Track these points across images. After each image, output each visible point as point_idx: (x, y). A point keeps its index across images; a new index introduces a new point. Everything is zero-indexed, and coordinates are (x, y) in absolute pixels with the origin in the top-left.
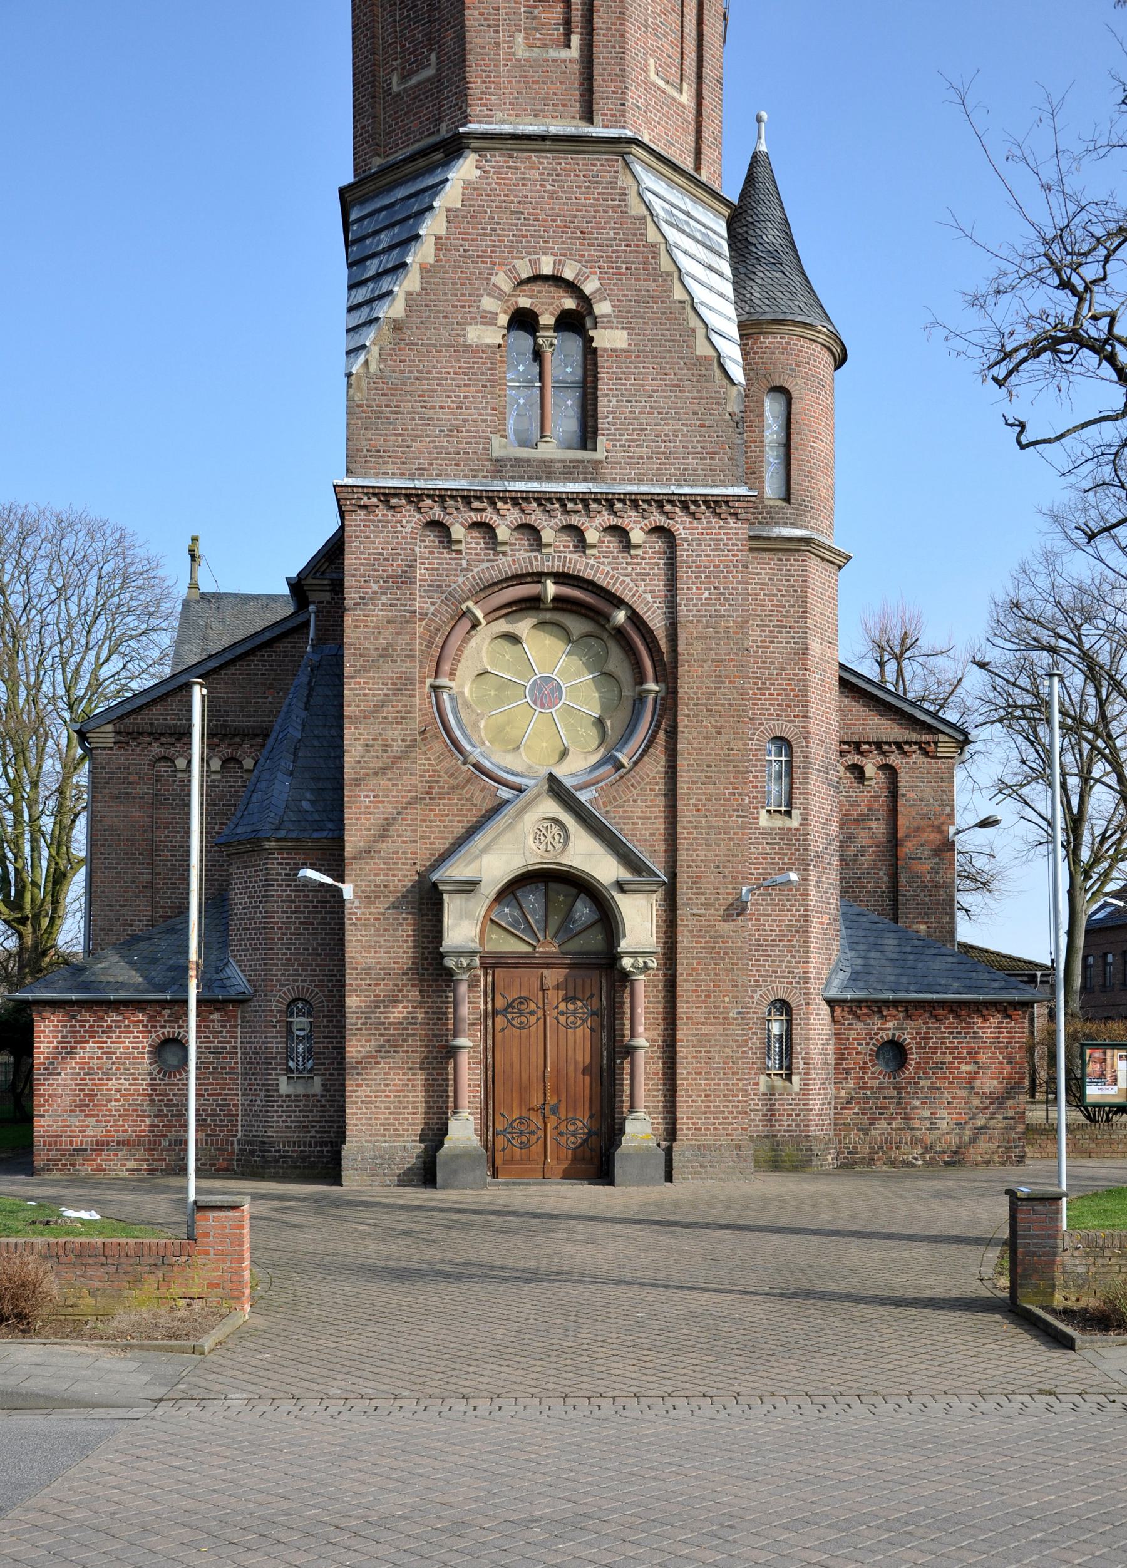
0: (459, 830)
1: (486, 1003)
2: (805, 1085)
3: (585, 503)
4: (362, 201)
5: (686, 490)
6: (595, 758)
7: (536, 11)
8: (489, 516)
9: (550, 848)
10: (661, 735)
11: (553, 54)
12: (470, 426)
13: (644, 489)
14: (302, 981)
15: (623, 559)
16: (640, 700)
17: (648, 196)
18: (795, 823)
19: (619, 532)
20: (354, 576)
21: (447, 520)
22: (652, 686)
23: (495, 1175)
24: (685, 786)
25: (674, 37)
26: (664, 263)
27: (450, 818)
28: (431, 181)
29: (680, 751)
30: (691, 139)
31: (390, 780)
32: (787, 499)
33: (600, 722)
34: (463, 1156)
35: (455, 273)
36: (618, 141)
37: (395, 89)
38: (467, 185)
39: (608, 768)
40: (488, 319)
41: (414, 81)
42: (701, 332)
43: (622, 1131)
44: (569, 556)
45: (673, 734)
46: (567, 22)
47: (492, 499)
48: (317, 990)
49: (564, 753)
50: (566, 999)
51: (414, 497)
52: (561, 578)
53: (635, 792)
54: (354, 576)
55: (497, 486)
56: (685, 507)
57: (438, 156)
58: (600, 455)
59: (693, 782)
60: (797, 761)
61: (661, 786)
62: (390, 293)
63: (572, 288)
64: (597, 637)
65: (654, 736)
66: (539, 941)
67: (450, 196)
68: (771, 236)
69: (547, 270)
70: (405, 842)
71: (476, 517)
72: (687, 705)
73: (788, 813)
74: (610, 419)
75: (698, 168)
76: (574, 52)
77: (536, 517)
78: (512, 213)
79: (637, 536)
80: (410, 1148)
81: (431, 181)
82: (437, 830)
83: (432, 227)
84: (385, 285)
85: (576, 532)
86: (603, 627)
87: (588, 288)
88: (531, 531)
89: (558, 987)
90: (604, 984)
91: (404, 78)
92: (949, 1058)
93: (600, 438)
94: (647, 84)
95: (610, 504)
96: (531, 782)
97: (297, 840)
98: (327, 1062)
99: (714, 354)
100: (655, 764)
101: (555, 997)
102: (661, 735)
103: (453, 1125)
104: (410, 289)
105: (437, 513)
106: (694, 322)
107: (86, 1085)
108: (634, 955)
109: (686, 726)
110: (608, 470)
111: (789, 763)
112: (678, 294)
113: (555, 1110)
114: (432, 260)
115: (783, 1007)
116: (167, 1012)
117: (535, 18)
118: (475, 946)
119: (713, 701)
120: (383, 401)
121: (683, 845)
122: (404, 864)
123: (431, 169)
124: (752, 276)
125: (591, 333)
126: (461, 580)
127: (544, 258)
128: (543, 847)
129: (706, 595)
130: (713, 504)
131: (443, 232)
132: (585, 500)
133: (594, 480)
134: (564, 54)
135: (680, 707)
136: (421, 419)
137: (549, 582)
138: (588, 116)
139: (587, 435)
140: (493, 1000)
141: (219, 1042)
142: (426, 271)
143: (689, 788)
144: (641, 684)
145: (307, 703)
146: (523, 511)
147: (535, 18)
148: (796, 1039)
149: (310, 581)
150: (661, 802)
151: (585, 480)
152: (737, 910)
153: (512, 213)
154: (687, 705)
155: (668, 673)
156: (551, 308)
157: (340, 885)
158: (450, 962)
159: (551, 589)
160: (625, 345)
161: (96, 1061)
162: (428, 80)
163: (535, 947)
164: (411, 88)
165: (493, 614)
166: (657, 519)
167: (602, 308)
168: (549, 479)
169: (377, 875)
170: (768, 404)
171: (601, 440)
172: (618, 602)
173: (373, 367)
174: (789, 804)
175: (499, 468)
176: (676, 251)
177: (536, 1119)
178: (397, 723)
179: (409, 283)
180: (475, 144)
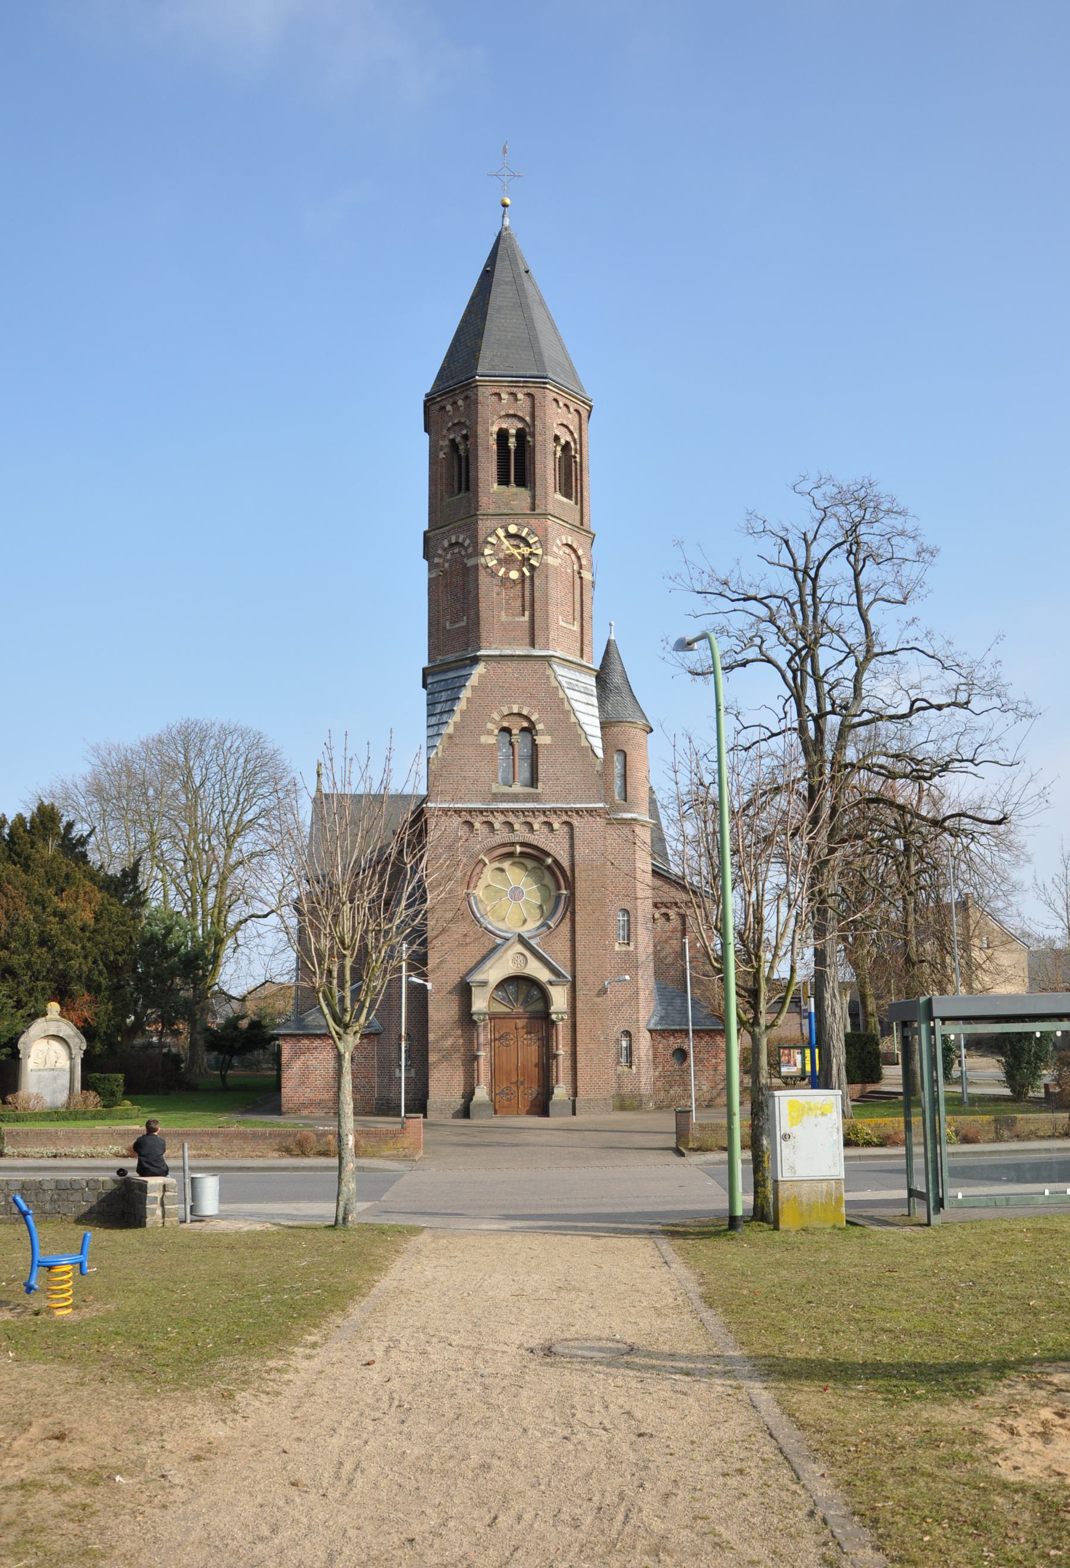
0: (479, 958)
3: (533, 812)
4: (434, 674)
5: (578, 806)
6: (538, 923)
8: (491, 819)
10: (568, 914)
11: (517, 619)
12: (482, 779)
13: (559, 805)
15: (550, 836)
16: (559, 897)
17: (560, 678)
18: (631, 948)
19: (549, 824)
21: (472, 820)
22: (564, 892)
23: (496, 1113)
25: (570, 603)
26: (567, 707)
28: (464, 673)
30: (579, 644)
32: (625, 800)
33: (541, 907)
34: (481, 1105)
36: (546, 656)
37: (448, 628)
38: (480, 676)
39: (545, 928)
40: (490, 733)
41: (457, 626)
42: (583, 736)
43: (553, 1093)
45: (573, 913)
46: (523, 606)
49: (525, 921)
50: (527, 1033)
51: (458, 811)
52: (522, 844)
55: (494, 806)
57: (468, 662)
58: (539, 790)
60: (632, 920)
61: (568, 936)
62: (447, 722)
63: (527, 718)
65: (565, 914)
67: (473, 681)
68: (616, 680)
69: (515, 711)
71: (485, 819)
73: (628, 944)
76: (526, 618)
77: (511, 818)
79: (556, 826)
80: (458, 1102)
81: (464, 673)
83: (465, 694)
84: (445, 718)
85: (529, 825)
87: (533, 718)
88: (510, 825)
89: (523, 1028)
91: (453, 623)
92: (706, 1056)
94: (560, 628)
95: (544, 812)
96: (509, 935)
100: (566, 927)
101: (522, 1032)
102: (568, 914)
103: (477, 1091)
105: (469, 818)
106: (580, 731)
108: (557, 1013)
111: (628, 921)
112: (573, 720)
113: (522, 1083)
115: (627, 1034)
118: (486, 1010)
121: (578, 963)
123: (464, 667)
130: (590, 811)
131: (470, 696)
132: (533, 811)
134: (522, 619)
139: (534, 781)
142: (462, 712)
148: (633, 1049)
150: (568, 943)
152: (603, 992)
155: (571, 885)
158: (475, 1017)
159: (519, 849)
165: (492, 861)
166: (565, 818)
167: (540, 727)
170: (616, 757)
171: (540, 784)
172: (548, 855)
173: (440, 755)
174: (629, 939)
175: (496, 797)
176: (572, 702)
177: (514, 1088)
179: (456, 717)
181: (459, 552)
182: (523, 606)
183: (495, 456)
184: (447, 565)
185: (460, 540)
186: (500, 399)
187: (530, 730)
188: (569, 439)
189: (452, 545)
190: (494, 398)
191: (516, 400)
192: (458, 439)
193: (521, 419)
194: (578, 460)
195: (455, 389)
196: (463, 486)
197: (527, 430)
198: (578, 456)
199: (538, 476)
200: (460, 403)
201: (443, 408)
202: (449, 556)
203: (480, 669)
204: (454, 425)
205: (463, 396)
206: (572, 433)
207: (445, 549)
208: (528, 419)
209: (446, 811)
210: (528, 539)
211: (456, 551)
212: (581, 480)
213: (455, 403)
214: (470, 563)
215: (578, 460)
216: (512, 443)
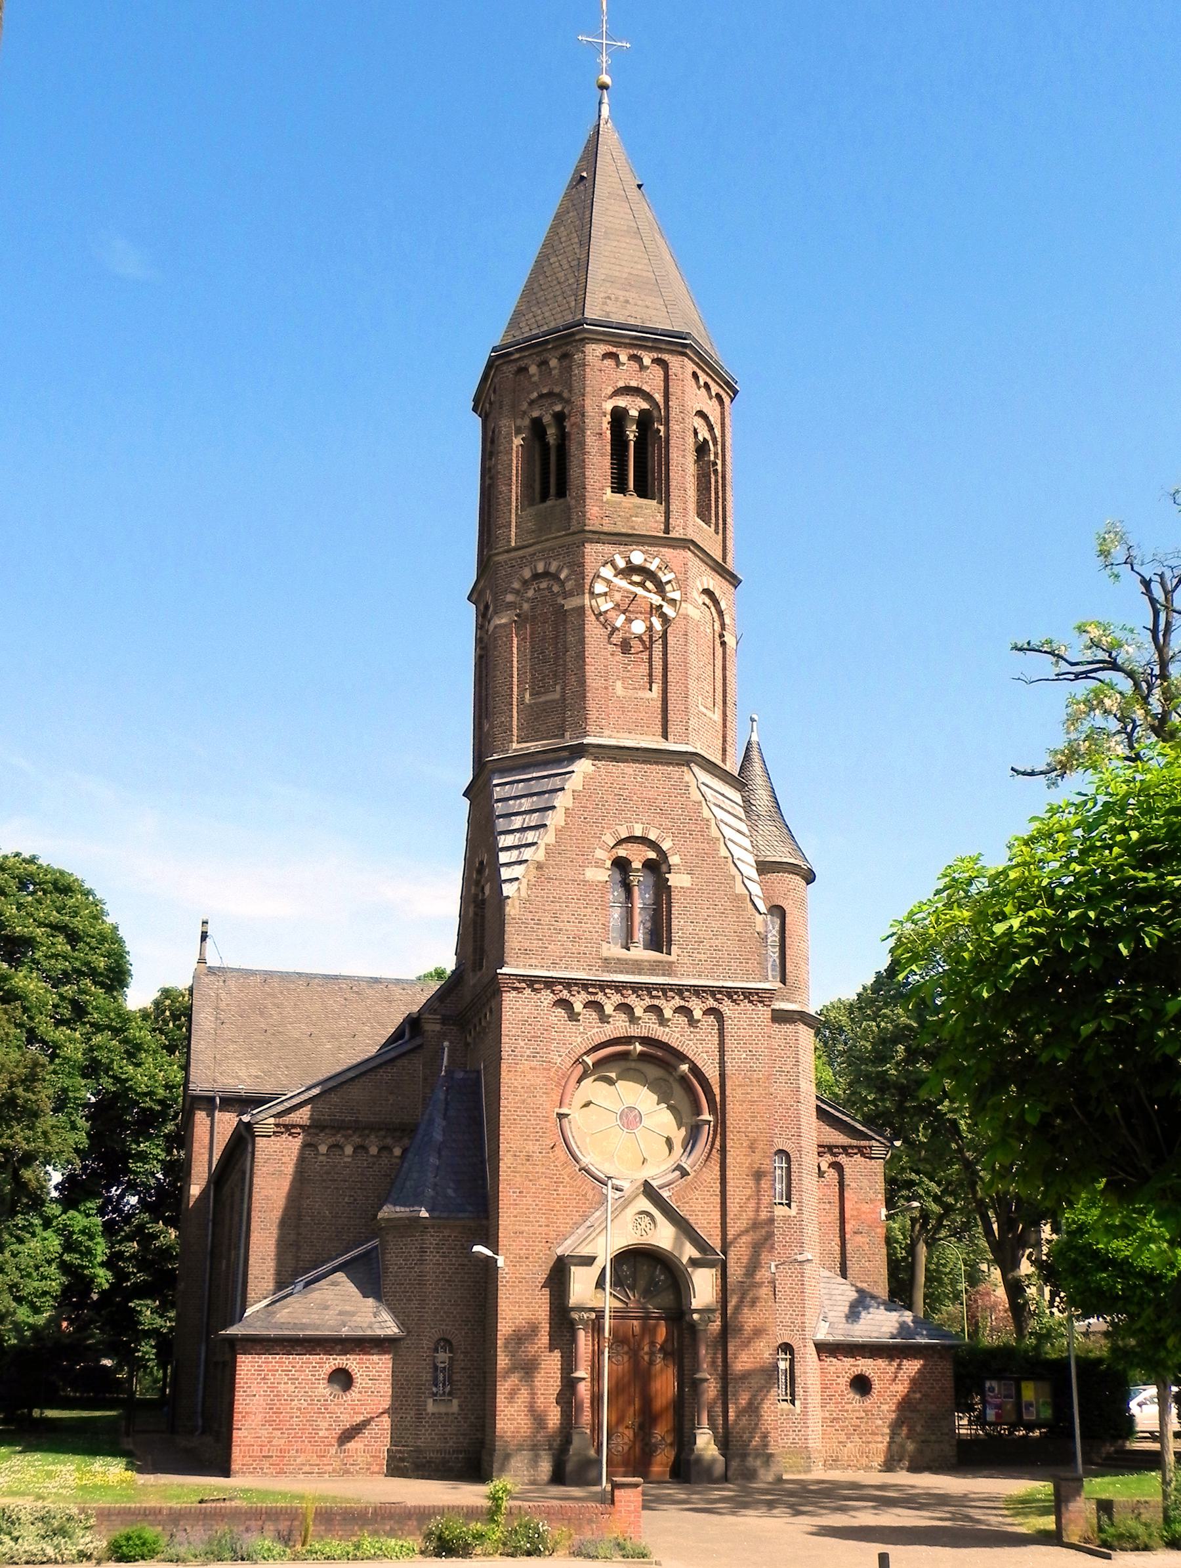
1: (593, 1345)
2: (805, 1406)
7: (629, 668)
8: (600, 997)
9: (644, 1233)
11: (641, 694)
12: (587, 935)
14: (447, 1325)
17: (703, 788)
18: (793, 1212)
20: (508, 1035)
21: (572, 999)
24: (732, 1189)
26: (714, 832)
27: (571, 1209)
29: (728, 1165)
31: (530, 1181)
32: (783, 981)
35: (578, 832)
39: (677, 1173)
40: (599, 864)
42: (739, 878)
44: (652, 1025)
45: (723, 1151)
46: (650, 675)
47: (603, 986)
48: (456, 1332)
52: (645, 1040)
53: (697, 1192)
54: (508, 1035)
56: (730, 997)
57: (565, 754)
58: (673, 958)
59: (738, 1187)
60: (794, 1167)
63: (653, 845)
64: (665, 1080)
66: (630, 1299)
67: (575, 782)
69: (638, 833)
70: (541, 1226)
72: (732, 1132)
73: (789, 1205)
74: (680, 934)
75: (724, 761)
77: (632, 1000)
78: (615, 795)
82: (561, 1217)
83: (562, 801)
84: (530, 836)
85: (656, 1010)
86: (671, 1074)
87: (665, 846)
90: (675, 1332)
93: (673, 946)
97: (447, 1218)
98: (463, 1387)
99: (747, 893)
104: (548, 842)
105: (565, 994)
107: (275, 1404)
109: (732, 1147)
110: (680, 969)
111: (789, 1169)
112: (723, 852)
114: (563, 824)
116: (339, 1347)
117: (628, 671)
119: (749, 1130)
120: (530, 916)
122: (540, 1242)
123: (558, 762)
124: (756, 828)
125: (667, 876)
126: (579, 1040)
127: (636, 825)
128: (639, 1232)
129: (744, 1056)
130: (748, 994)
131: (570, 805)
132: (664, 989)
133: (669, 975)
134: (648, 694)
135: (728, 1133)
136: (555, 929)
137: (637, 1044)
138: (665, 736)
139: (659, 939)
140: (598, 1343)
141: (377, 1372)
142: (558, 831)
143: (734, 1191)
144: (699, 1115)
145: (445, 1115)
146: (622, 995)
147: (628, 671)
149: (427, 1016)
151: (664, 975)
153: (615, 795)
154: (732, 1132)
155: (720, 1110)
156: (640, 858)
157: (496, 1256)
158: (575, 1315)
159: (639, 1048)
160: (689, 885)
161: (282, 1385)
162: (553, 701)
163: (627, 1304)
164: (540, 703)
166: (711, 1003)
167: (674, 860)
168: (640, 974)
169: (521, 1249)
172: (683, 1058)
174: (789, 1198)
178: (537, 1140)
180: (593, 750)
181: (549, 588)
182: (650, 675)
183: (609, 448)
184: (526, 606)
185: (553, 569)
186: (618, 363)
187: (657, 868)
188: (708, 437)
189: (536, 576)
190: (609, 363)
191: (642, 367)
192: (547, 419)
193: (647, 397)
194: (719, 468)
195: (547, 342)
196: (553, 490)
197: (655, 413)
198: (719, 462)
199: (673, 483)
200: (553, 363)
201: (523, 370)
202: (530, 593)
203: (583, 767)
204: (541, 396)
205: (558, 353)
206: (711, 428)
207: (525, 583)
208: (659, 397)
209: (532, 982)
210: (660, 574)
211: (544, 585)
212: (724, 499)
213: (544, 363)
214: (570, 603)
215: (719, 468)
216: (632, 432)
